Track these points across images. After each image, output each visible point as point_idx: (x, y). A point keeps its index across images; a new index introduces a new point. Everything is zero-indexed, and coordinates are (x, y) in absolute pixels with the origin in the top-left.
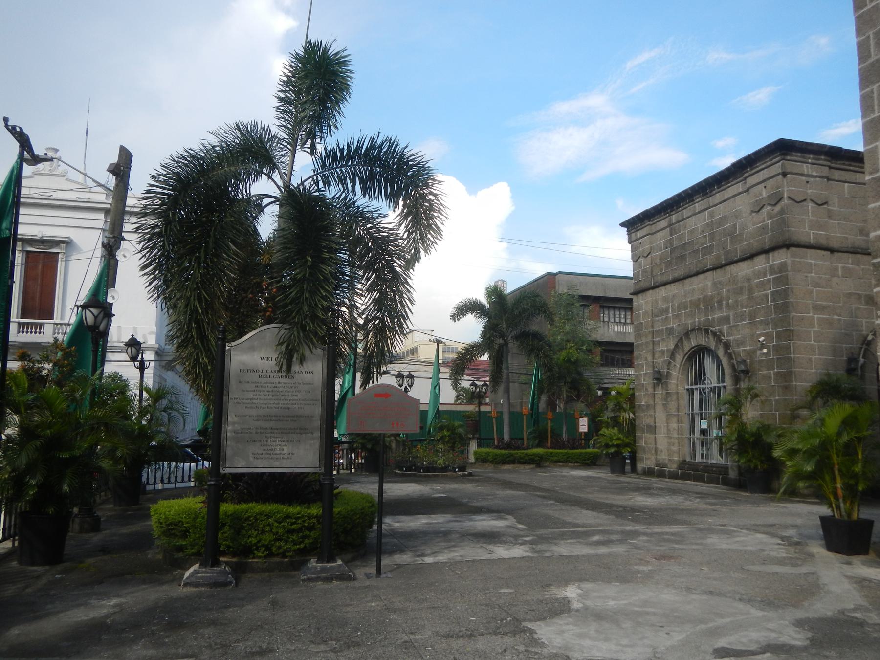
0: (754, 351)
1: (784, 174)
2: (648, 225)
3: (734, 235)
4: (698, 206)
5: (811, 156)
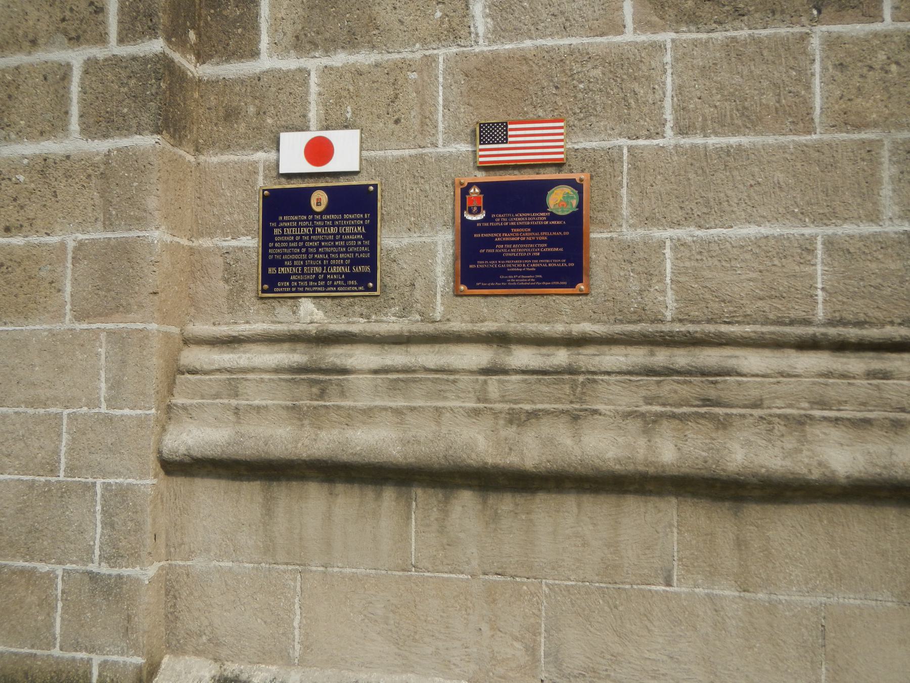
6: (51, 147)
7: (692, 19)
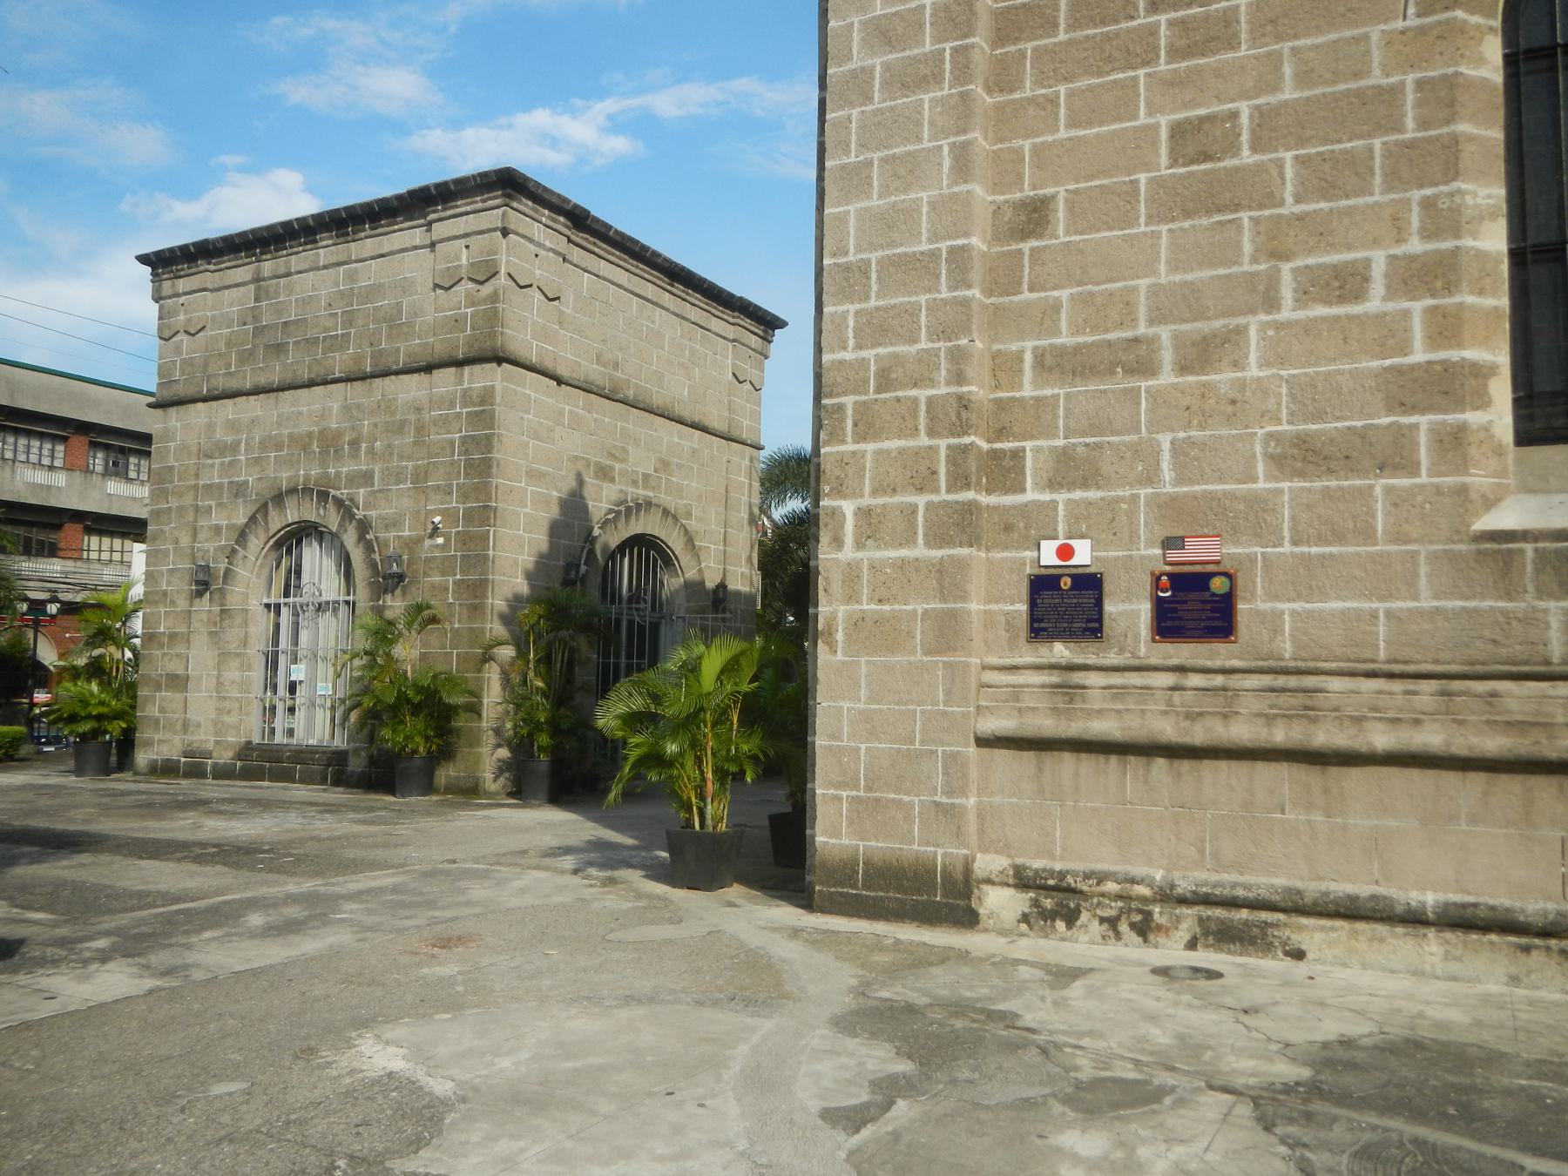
0: (419, 541)
1: (505, 232)
3: (394, 322)
5: (546, 212)
6: (904, 553)
7: (1302, 475)
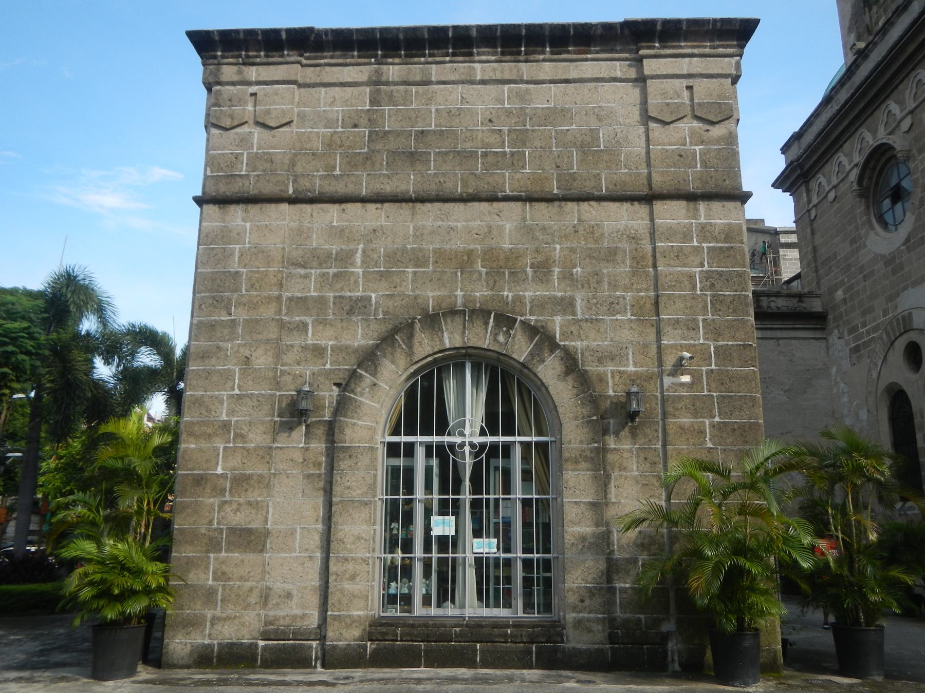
2: (299, 62)
4: (479, 70)
